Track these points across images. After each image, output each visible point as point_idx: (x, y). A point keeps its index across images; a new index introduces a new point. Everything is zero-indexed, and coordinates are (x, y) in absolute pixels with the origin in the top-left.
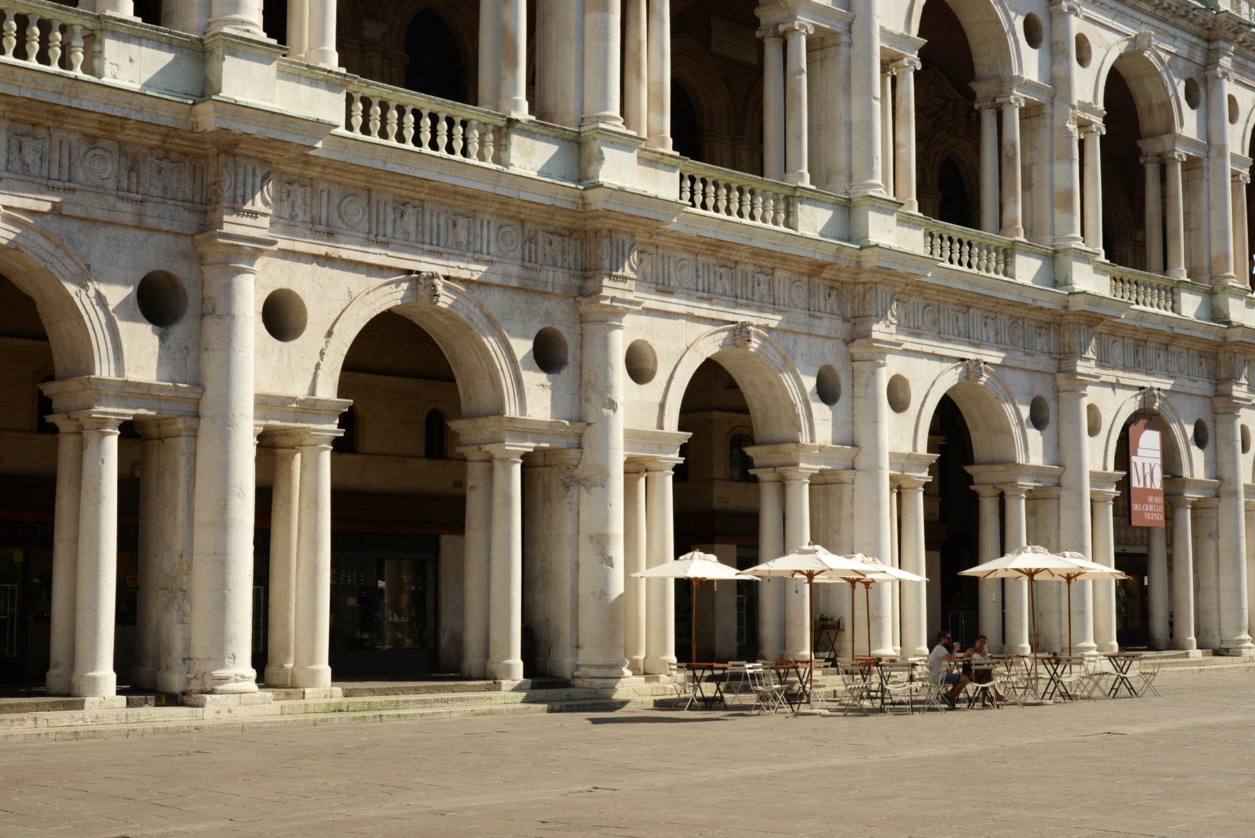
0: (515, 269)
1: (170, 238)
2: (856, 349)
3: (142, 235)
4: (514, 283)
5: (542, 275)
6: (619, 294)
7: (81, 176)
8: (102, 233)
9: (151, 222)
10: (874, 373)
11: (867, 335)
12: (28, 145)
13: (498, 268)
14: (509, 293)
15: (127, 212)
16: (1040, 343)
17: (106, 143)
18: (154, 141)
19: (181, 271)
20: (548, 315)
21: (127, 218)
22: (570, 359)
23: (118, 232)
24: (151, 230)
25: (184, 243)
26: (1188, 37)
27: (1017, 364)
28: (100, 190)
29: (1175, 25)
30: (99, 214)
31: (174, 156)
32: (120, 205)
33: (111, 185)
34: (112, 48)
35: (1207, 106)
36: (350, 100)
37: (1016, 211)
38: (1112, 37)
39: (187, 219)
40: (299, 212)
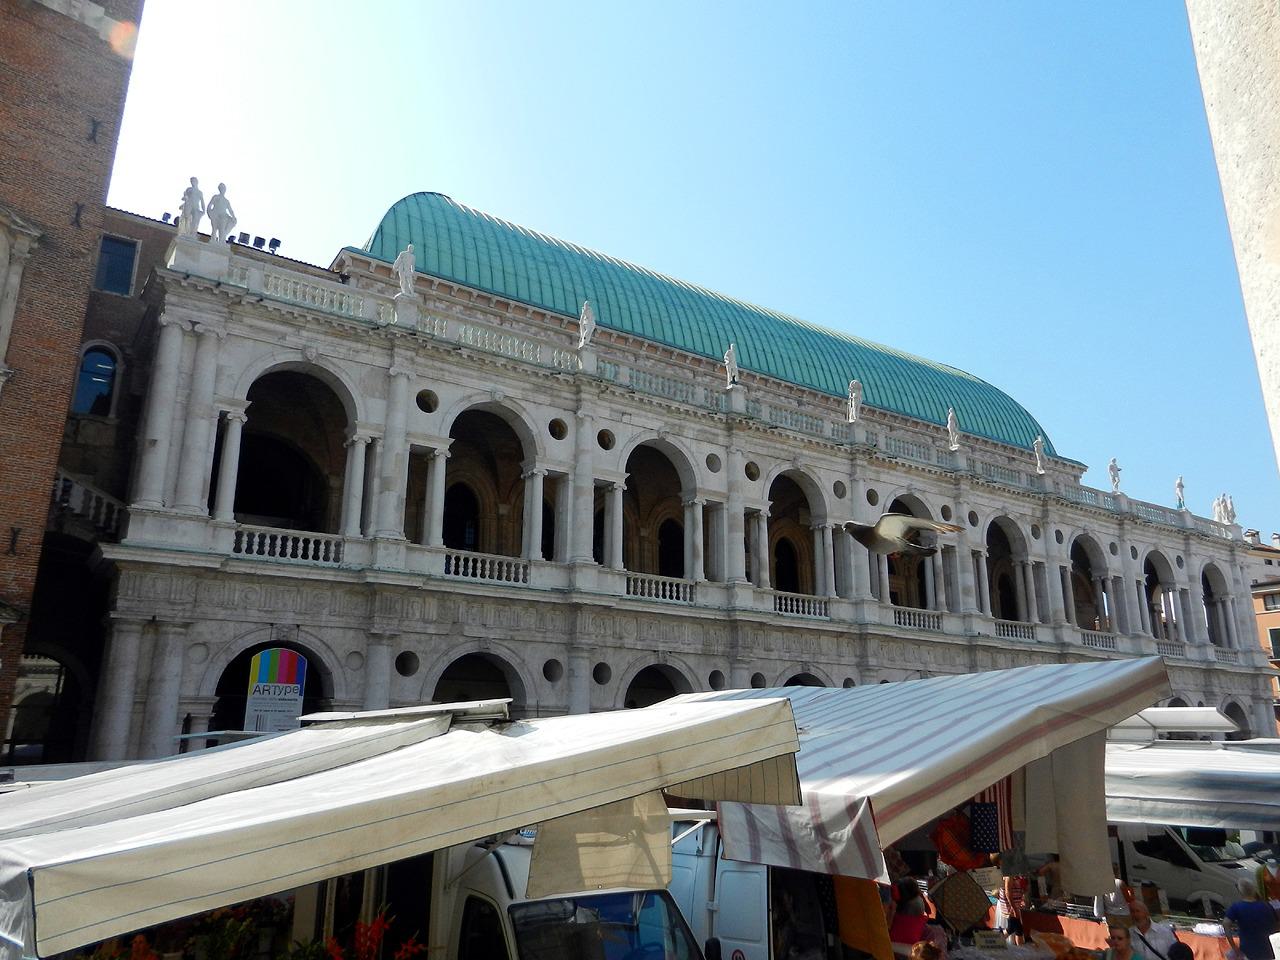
0: (700, 646)
1: (555, 646)
3: (545, 645)
8: (530, 646)
9: (548, 640)
15: (539, 637)
19: (562, 658)
20: (715, 665)
21: (539, 639)
23: (535, 645)
26: (1031, 506)
28: (529, 629)
29: (1023, 501)
30: (528, 639)
32: (537, 634)
33: (534, 627)
34: (533, 572)
35: (1045, 537)
36: (628, 580)
37: (942, 598)
38: (988, 510)
40: (608, 630)
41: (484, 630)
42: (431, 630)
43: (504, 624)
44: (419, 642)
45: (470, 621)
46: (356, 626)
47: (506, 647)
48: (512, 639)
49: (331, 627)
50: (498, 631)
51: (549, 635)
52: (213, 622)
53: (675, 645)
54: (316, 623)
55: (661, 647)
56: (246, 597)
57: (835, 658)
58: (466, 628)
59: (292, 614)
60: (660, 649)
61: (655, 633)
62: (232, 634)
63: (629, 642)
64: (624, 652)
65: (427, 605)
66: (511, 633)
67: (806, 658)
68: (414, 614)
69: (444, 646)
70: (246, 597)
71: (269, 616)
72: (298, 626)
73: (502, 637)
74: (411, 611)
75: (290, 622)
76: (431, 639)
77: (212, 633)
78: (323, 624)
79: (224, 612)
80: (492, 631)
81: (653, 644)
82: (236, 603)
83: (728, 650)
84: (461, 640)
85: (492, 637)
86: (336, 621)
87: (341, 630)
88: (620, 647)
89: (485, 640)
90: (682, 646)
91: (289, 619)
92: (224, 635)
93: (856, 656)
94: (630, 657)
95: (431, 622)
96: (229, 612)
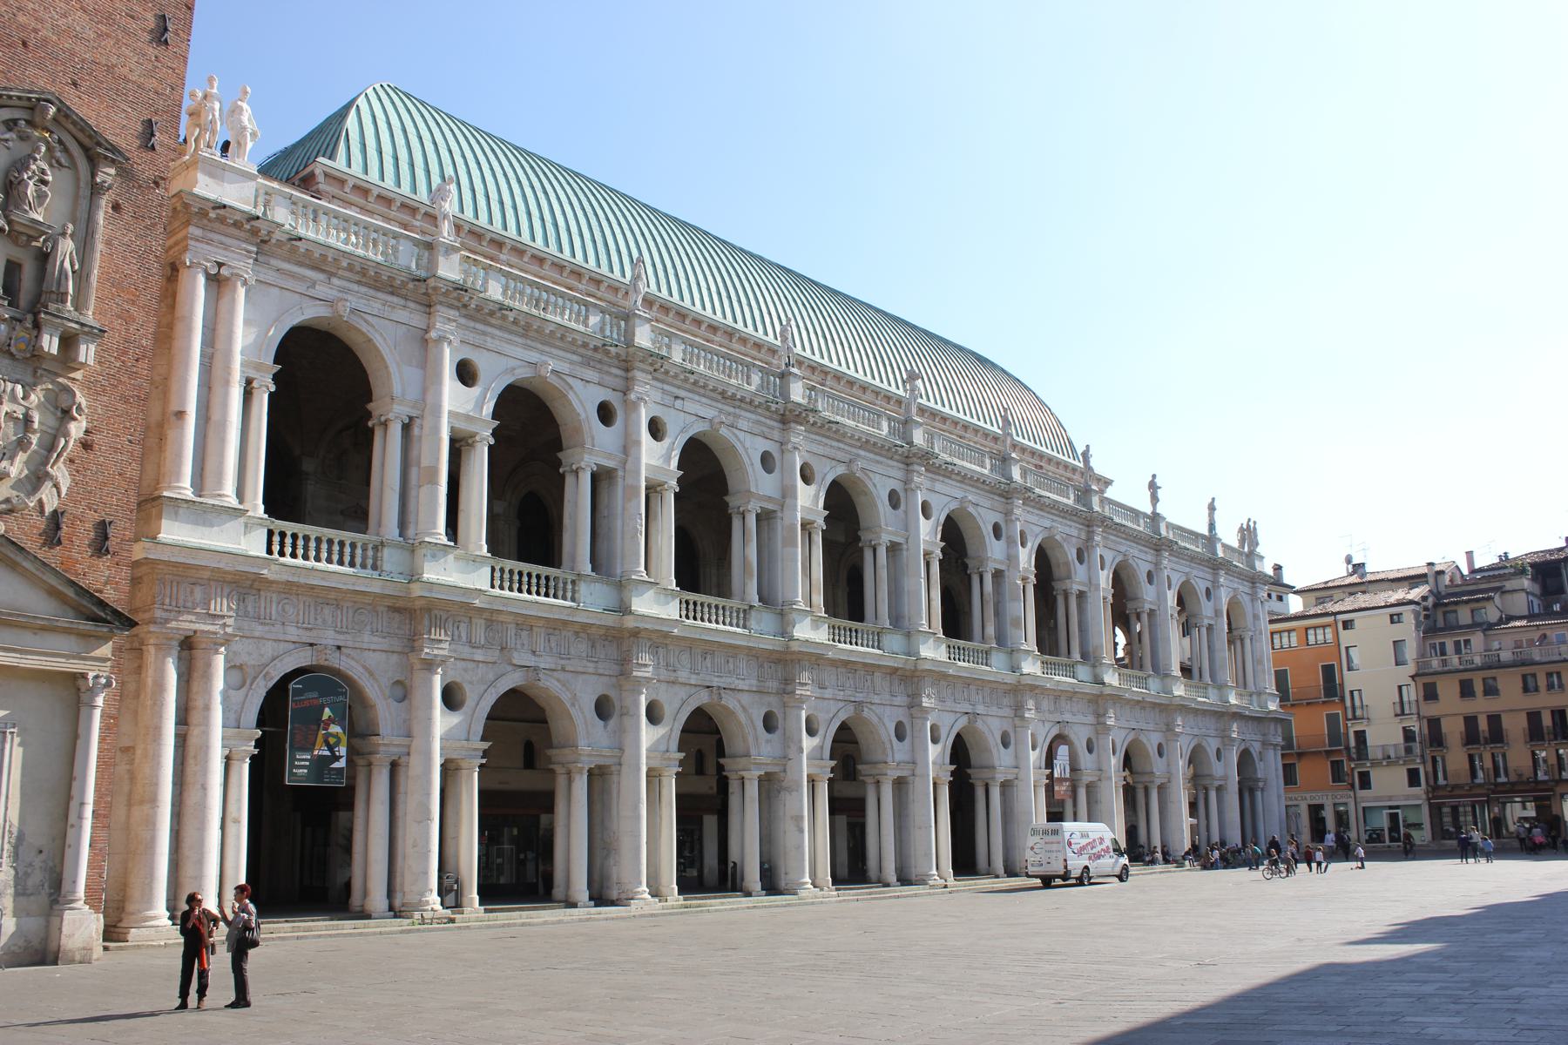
0: (754, 682)
2: (914, 711)
3: (596, 677)
4: (754, 689)
5: (767, 684)
6: (803, 692)
7: (573, 652)
8: (581, 677)
9: (601, 671)
10: (923, 724)
11: (920, 705)
12: (552, 638)
13: (747, 682)
14: (752, 694)
15: (591, 667)
16: (1006, 701)
17: (582, 635)
18: (602, 632)
19: (612, 694)
21: (591, 670)
22: (779, 726)
24: (600, 675)
25: (614, 680)
27: (994, 714)
30: (580, 669)
31: (610, 638)
33: (584, 655)
39: (615, 669)
40: (661, 661)
41: (533, 658)
42: (479, 655)
43: (555, 651)
44: (466, 670)
45: (519, 646)
46: (399, 649)
47: (558, 680)
48: (563, 670)
49: (374, 650)
50: (549, 659)
51: (600, 665)
52: (250, 640)
53: (729, 680)
54: (357, 645)
55: (716, 682)
56: (283, 610)
57: (888, 697)
58: (515, 654)
59: (332, 632)
60: (715, 684)
61: (709, 665)
62: (270, 655)
63: (683, 675)
64: (677, 688)
65: (474, 626)
66: (563, 662)
67: (860, 697)
68: (459, 636)
69: (491, 677)
70: (283, 610)
71: (308, 633)
72: (339, 648)
73: (553, 666)
74: (456, 633)
75: (331, 642)
76: (478, 667)
77: (249, 654)
78: (365, 646)
79: (260, 628)
80: (541, 659)
81: (708, 678)
82: (273, 618)
83: (782, 686)
84: (510, 668)
85: (542, 666)
86: (378, 642)
87: (384, 655)
88: (673, 682)
89: (536, 669)
90: (737, 682)
91: (329, 637)
92: (262, 655)
93: (908, 696)
94: (682, 693)
95: (478, 648)
96: (267, 628)
